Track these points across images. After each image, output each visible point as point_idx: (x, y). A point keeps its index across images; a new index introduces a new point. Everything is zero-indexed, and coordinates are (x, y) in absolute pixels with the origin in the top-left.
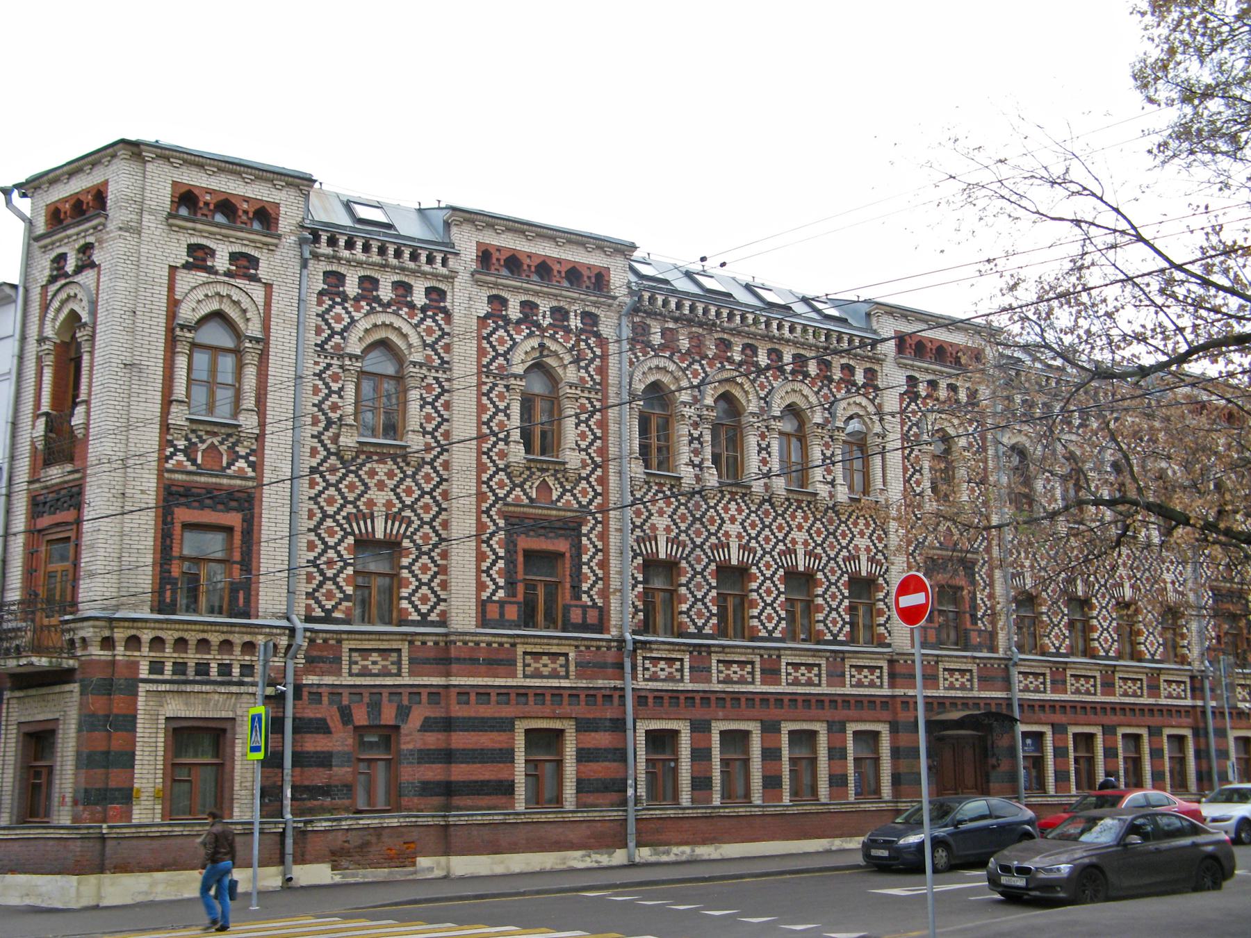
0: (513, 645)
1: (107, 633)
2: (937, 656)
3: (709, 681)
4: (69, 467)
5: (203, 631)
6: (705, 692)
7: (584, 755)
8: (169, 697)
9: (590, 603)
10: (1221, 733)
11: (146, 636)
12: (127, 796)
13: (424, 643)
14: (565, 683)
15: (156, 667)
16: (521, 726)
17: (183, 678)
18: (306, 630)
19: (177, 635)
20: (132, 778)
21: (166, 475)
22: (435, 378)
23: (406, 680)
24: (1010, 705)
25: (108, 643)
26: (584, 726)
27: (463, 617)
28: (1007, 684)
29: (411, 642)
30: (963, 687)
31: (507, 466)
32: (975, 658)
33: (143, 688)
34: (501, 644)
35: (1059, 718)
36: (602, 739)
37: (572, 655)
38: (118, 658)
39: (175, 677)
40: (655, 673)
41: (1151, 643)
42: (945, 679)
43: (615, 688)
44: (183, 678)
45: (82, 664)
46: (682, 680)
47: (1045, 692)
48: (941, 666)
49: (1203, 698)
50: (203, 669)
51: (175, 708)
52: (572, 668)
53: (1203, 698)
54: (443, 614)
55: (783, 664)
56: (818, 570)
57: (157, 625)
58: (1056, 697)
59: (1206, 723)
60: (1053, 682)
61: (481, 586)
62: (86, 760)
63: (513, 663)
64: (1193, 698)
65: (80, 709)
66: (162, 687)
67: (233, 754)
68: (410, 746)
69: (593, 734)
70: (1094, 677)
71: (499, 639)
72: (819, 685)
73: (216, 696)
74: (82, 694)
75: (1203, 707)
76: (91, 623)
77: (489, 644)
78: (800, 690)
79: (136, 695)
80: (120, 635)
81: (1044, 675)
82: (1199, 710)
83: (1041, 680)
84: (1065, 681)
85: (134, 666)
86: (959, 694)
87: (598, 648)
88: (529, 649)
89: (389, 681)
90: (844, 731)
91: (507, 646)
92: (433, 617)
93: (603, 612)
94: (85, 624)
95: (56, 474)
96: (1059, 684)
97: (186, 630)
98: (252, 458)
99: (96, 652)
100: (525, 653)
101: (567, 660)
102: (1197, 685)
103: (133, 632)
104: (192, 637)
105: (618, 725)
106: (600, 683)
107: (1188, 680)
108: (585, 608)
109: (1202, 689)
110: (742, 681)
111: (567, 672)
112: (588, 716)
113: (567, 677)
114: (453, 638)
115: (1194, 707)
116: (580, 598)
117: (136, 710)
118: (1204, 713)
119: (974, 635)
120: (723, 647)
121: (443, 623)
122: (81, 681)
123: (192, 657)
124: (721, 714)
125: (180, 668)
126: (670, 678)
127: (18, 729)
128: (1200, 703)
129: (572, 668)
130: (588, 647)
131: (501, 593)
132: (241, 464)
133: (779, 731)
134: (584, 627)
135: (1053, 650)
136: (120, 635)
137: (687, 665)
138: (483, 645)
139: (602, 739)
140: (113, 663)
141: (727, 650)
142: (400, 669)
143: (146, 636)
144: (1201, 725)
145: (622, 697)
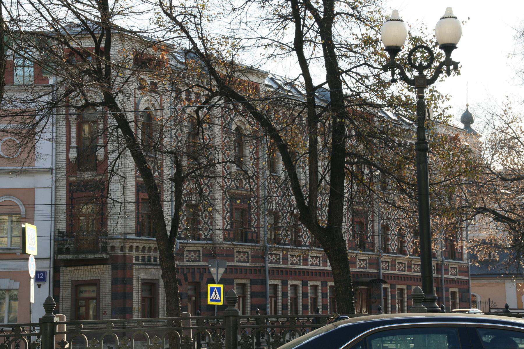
0: (233, 248)
1: (122, 245)
2: (357, 253)
3: (287, 264)
4: (95, 173)
5: (150, 244)
6: (286, 268)
7: (253, 295)
8: (141, 270)
9: (254, 231)
10: (447, 290)
11: (135, 246)
12: (131, 310)
13: (206, 247)
14: (248, 264)
15: (137, 259)
16: (237, 281)
17: (144, 262)
18: (180, 243)
19: (143, 245)
20: (132, 303)
21: (138, 179)
22: (208, 135)
23: (202, 263)
24: (379, 276)
25: (122, 249)
26: (253, 282)
27: (219, 237)
28: (378, 267)
29: (203, 247)
30: (363, 268)
31: (230, 172)
32: (368, 254)
33: (135, 266)
34: (230, 248)
35: (393, 282)
36: (258, 288)
37: (250, 253)
38: (127, 255)
39: (142, 263)
40: (272, 260)
41: (393, 245)
42: (237, 257)
43: (262, 267)
44: (144, 262)
45: (111, 257)
46: (279, 263)
47: (388, 270)
48: (357, 258)
49: (441, 274)
50: (149, 259)
51: (143, 275)
52: (250, 258)
53: (441, 274)
54: (211, 235)
55: (289, 256)
56: (320, 216)
57: (139, 241)
58: (393, 272)
59: (442, 285)
60: (392, 265)
61: (224, 224)
62: (114, 296)
63: (233, 256)
64: (437, 274)
65: (112, 275)
66: (140, 267)
67: (159, 293)
68: (204, 291)
69: (256, 286)
70: (405, 263)
71: (229, 246)
72: (319, 266)
73: (153, 270)
74: (112, 269)
75: (441, 277)
76: (118, 240)
77: (227, 248)
78: (314, 268)
79: (132, 270)
80: (128, 245)
81: (388, 262)
82: (439, 279)
83: (318, 260)
84: (395, 265)
85: (131, 257)
86: (362, 270)
87: (257, 249)
88: (238, 250)
89: (197, 263)
90: (326, 286)
91: (231, 249)
92: (209, 237)
93: (258, 234)
94: (115, 241)
95: (87, 176)
96: (393, 267)
97: (146, 243)
98: (159, 171)
99: (120, 253)
100: (237, 252)
101: (248, 255)
102: (439, 267)
103: (131, 244)
104: (147, 246)
105: (264, 282)
106: (258, 265)
107: (435, 265)
108: (252, 232)
109: (441, 269)
110: (297, 264)
111: (248, 259)
112: (255, 278)
113: (248, 262)
114: (217, 246)
115: (437, 277)
116: (250, 229)
117: (133, 276)
118: (441, 280)
119: (367, 245)
120: (293, 249)
121: (211, 239)
122: (111, 264)
123: (147, 254)
124: (291, 278)
125: (143, 258)
126: (276, 263)
127: (72, 283)
128: (440, 276)
129: (250, 258)
130: (254, 249)
131: (229, 227)
132: (156, 173)
133: (308, 286)
134: (252, 241)
135: (392, 251)
136: (128, 245)
137: (281, 256)
138: (255, 250)
139: (258, 288)
140: (125, 257)
141: (293, 250)
142: (199, 258)
143: (135, 246)
144: (440, 286)
145: (265, 270)
